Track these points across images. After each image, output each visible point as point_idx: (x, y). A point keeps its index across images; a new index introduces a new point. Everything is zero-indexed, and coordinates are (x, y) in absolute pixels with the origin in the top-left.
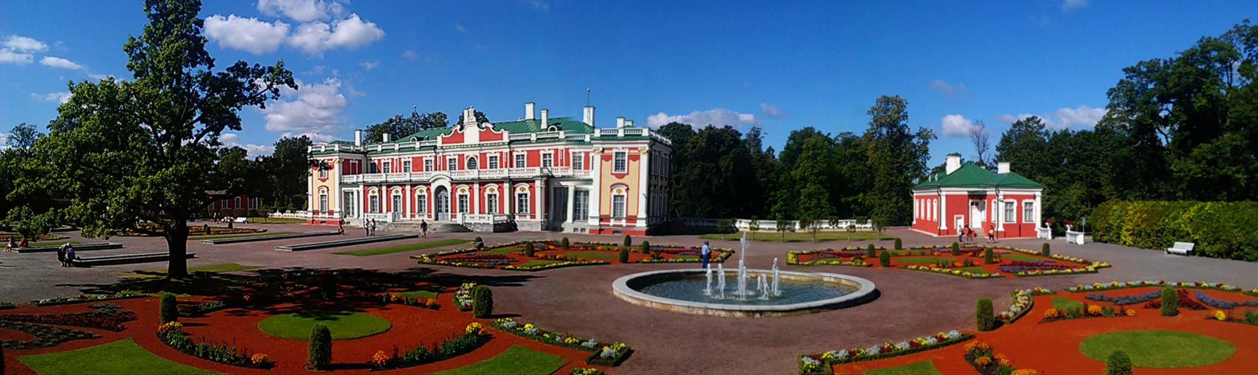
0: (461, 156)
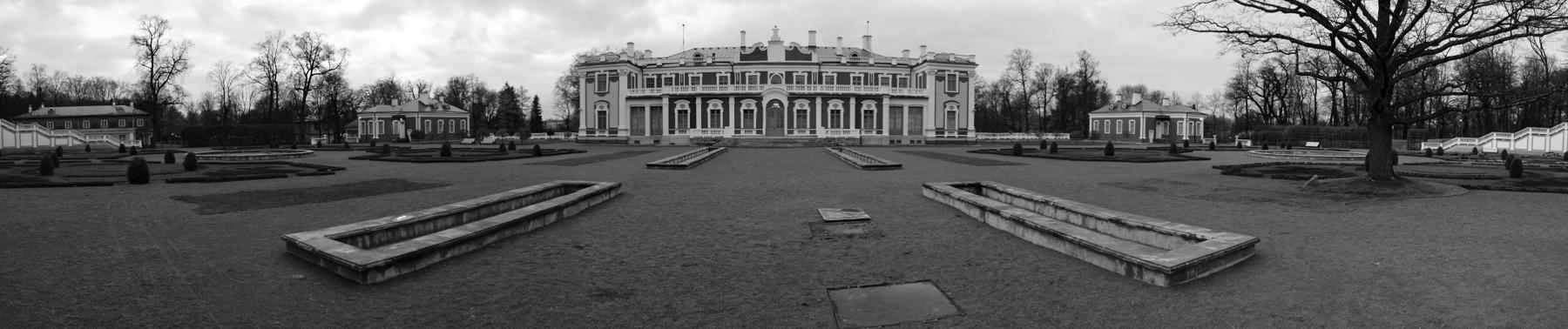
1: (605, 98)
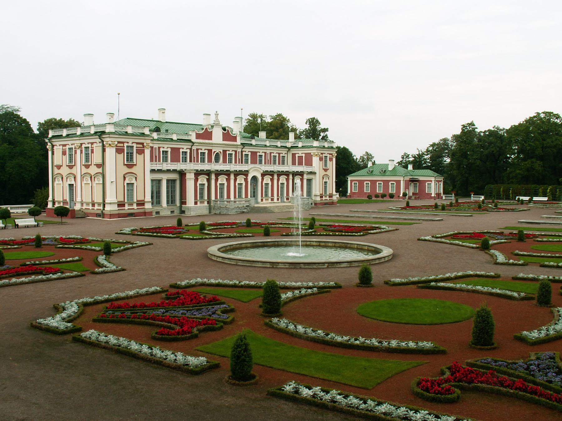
0: (210, 151)
1: (133, 170)
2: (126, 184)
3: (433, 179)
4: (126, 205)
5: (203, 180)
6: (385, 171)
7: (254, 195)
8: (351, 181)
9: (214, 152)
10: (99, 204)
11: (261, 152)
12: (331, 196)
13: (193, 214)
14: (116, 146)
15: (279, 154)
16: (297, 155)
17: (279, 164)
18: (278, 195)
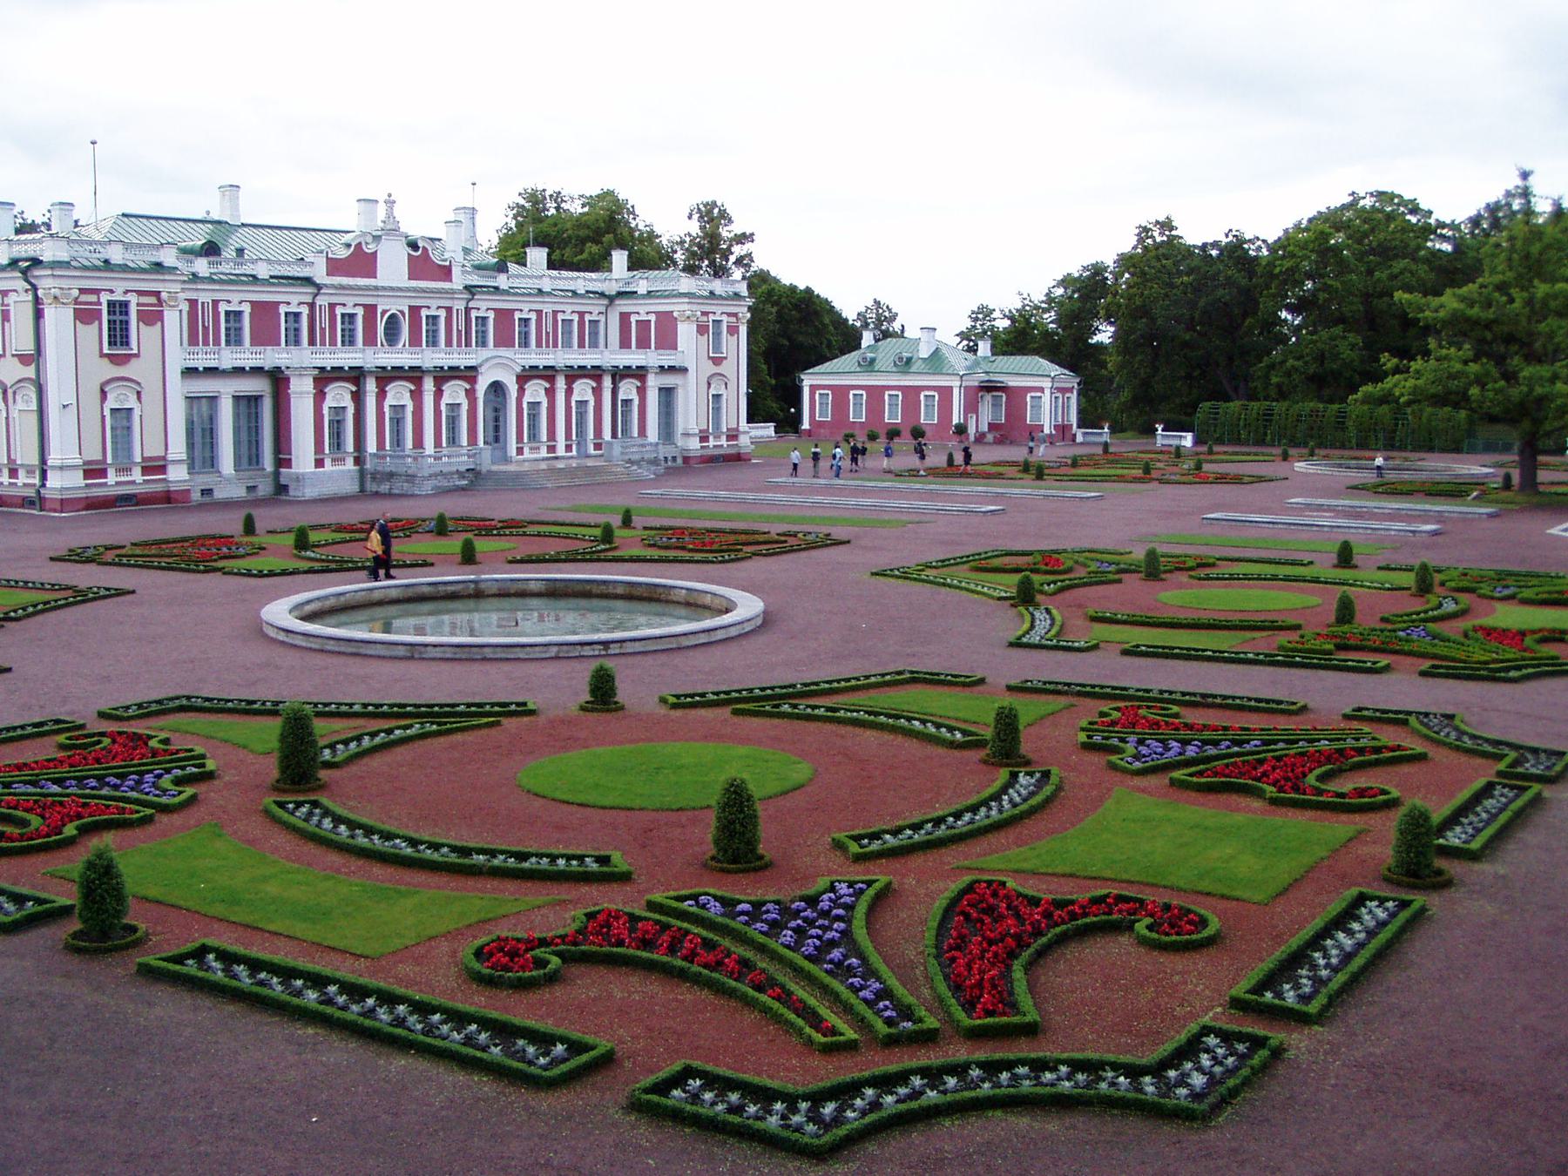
0: (370, 310)
2: (107, 413)
3: (1047, 384)
4: (111, 472)
5: (339, 395)
6: (909, 360)
7: (497, 435)
8: (813, 388)
9: (384, 312)
10: (30, 472)
11: (525, 309)
12: (733, 436)
13: (310, 492)
14: (76, 301)
15: (581, 314)
16: (633, 319)
17: (581, 345)
18: (568, 436)
